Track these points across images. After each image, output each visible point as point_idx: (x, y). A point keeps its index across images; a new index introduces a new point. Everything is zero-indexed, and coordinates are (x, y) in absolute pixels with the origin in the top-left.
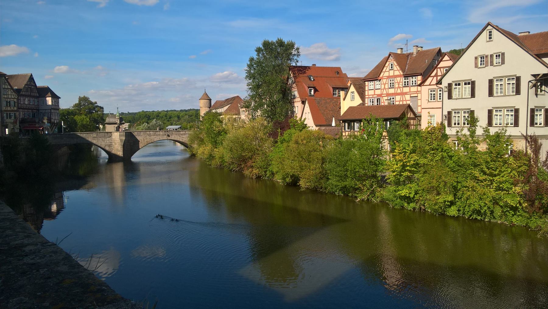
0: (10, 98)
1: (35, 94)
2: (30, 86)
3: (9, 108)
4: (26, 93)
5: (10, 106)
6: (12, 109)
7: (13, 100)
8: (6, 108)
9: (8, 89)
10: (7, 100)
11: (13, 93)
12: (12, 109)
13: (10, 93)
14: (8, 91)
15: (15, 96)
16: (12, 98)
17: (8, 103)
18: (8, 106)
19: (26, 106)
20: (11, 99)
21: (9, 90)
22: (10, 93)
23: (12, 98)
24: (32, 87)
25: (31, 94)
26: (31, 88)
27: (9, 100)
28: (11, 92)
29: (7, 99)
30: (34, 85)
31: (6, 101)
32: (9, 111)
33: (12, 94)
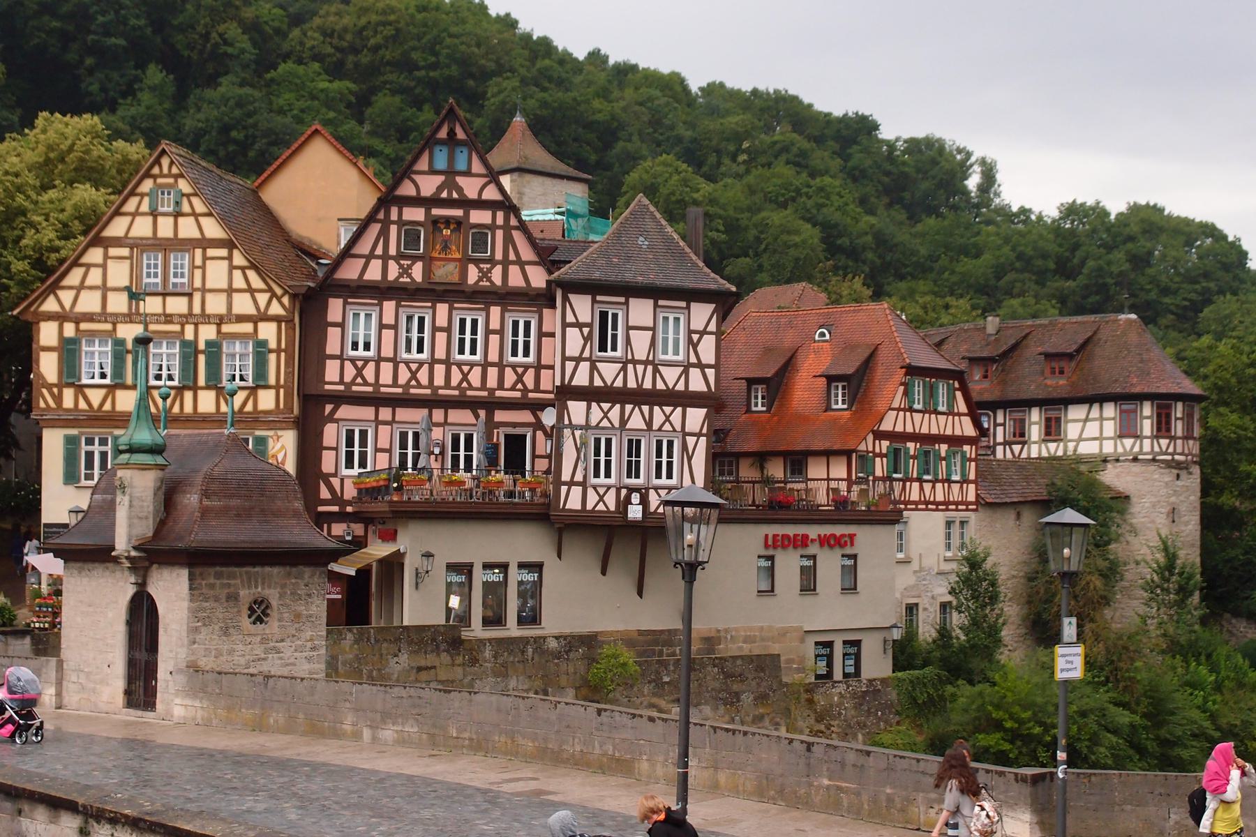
0: (220, 321)
1: (514, 270)
2: (458, 213)
5: (214, 383)
7: (247, 328)
9: (205, 243)
10: (189, 333)
11: (252, 274)
13: (217, 274)
14: (205, 258)
15: (263, 298)
16: (241, 319)
17: (202, 359)
18: (202, 381)
20: (226, 328)
21: (211, 252)
23: (241, 319)
25: (464, 273)
26: (459, 224)
27: (208, 333)
28: (232, 268)
30: (491, 194)
31: (185, 344)
33: (239, 282)
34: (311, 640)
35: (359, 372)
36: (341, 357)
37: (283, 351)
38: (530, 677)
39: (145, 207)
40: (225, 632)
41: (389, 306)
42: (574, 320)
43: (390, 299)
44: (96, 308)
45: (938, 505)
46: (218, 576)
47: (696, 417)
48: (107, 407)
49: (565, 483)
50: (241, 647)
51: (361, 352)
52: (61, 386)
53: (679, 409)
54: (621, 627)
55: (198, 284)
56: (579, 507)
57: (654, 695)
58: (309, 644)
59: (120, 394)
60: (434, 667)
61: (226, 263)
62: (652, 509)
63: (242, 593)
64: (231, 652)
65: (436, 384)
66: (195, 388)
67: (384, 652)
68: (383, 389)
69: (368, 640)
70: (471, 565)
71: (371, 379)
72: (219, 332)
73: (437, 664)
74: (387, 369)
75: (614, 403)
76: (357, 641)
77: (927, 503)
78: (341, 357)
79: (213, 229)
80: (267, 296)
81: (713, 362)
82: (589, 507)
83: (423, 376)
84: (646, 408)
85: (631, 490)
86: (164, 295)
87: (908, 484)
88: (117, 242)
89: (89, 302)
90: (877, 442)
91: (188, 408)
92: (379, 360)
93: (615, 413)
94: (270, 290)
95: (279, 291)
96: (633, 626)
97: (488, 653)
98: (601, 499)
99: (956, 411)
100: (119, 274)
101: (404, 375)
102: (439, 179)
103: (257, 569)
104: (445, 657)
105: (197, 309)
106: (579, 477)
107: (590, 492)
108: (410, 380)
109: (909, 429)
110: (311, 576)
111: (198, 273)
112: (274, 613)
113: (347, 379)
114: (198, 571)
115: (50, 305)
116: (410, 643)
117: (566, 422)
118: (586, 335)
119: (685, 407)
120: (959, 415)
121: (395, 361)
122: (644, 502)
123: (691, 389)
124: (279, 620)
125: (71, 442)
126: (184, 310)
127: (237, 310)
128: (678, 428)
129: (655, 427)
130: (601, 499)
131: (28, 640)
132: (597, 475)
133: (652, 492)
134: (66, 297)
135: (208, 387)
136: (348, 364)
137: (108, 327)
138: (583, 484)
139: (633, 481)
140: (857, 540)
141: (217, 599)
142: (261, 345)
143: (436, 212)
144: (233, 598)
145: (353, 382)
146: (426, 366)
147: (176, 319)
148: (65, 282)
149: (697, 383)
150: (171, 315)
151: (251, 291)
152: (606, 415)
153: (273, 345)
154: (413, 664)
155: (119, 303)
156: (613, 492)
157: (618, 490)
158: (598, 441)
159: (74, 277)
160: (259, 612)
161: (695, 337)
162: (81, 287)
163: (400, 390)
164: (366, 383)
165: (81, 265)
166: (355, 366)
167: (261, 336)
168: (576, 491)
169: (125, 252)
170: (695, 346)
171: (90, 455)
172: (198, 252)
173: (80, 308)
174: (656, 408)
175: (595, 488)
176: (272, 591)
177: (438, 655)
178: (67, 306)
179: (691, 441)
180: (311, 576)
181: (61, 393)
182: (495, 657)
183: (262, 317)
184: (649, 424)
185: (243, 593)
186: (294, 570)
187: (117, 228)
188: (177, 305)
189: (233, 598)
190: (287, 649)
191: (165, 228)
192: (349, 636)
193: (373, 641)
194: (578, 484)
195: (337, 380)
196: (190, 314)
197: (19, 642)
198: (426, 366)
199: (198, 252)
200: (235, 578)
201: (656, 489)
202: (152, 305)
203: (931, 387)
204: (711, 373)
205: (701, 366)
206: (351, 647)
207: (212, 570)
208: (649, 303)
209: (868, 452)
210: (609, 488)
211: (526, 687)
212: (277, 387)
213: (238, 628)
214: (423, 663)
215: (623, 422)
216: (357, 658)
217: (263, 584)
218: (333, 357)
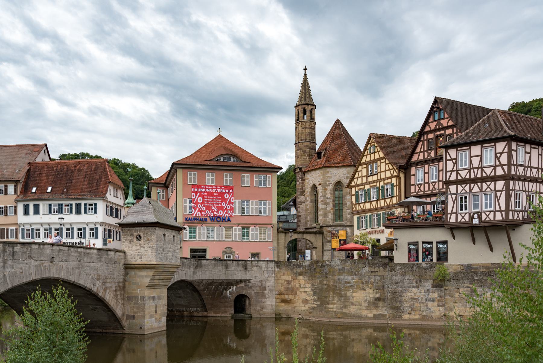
0: (384, 180)
3: (382, 202)
4: (429, 154)
6: (388, 203)
7: (389, 181)
8: (377, 203)
11: (390, 165)
12: (388, 203)
13: (383, 167)
14: (381, 163)
15: (392, 171)
16: (388, 178)
19: (431, 189)
20: (386, 182)
22: (383, 167)
23: (388, 178)
24: (449, 131)
27: (382, 184)
28: (386, 164)
29: (378, 183)
32: (381, 208)
34: (152, 245)
35: (420, 188)
36: (414, 185)
37: (397, 185)
38: (414, 276)
39: (368, 153)
40: (130, 242)
41: (427, 166)
42: (450, 158)
43: (427, 164)
44: (361, 183)
46: (128, 230)
47: (500, 184)
48: (364, 208)
49: (449, 214)
50: (134, 246)
51: (420, 182)
52: (356, 204)
53: (493, 183)
55: (379, 171)
56: (454, 221)
58: (151, 246)
59: (366, 204)
60: (377, 272)
61: (384, 163)
62: (483, 219)
63: (134, 234)
64: (132, 247)
65: (440, 188)
66: (380, 200)
67: (360, 267)
68: (426, 192)
69: (355, 263)
71: (423, 190)
72: (384, 183)
73: (378, 270)
74: (427, 185)
75: (467, 184)
76: (351, 263)
78: (414, 185)
79: (382, 155)
80: (393, 170)
81: (507, 163)
82: (459, 220)
83: (436, 186)
84: (479, 184)
85: (474, 213)
86: (373, 175)
88: (364, 164)
89: (359, 182)
91: (379, 206)
92: (425, 183)
93: (467, 188)
94: (394, 168)
95: (395, 168)
97: (398, 268)
98: (463, 217)
100: (365, 172)
101: (431, 187)
102: (436, 123)
103: (138, 228)
104: (381, 269)
105: (379, 178)
106: (454, 211)
107: (459, 215)
108: (433, 188)
110: (152, 229)
111: (379, 167)
112: (142, 238)
113: (417, 191)
114: (124, 229)
115: (353, 184)
116: (369, 264)
117: (449, 193)
118: (454, 162)
121: (429, 183)
122: (480, 217)
123: (497, 174)
124: (144, 240)
125: (358, 218)
126: (377, 179)
127: (387, 176)
128: (493, 189)
129: (484, 190)
130: (463, 217)
131: (274, 263)
132: (462, 209)
133: (483, 214)
134: (355, 180)
135: (382, 199)
136: (416, 186)
137: (363, 187)
138: (456, 213)
139: (476, 210)
141: (128, 235)
142: (392, 184)
143: (437, 133)
144: (132, 235)
145: (418, 192)
146: (437, 183)
147: (375, 181)
148: (355, 177)
149: (500, 172)
150: (374, 181)
151: (390, 170)
152: (464, 189)
153: (395, 184)
154: (370, 270)
155: (365, 180)
156: (467, 215)
157: (470, 214)
158: (461, 198)
159: (356, 176)
160: (139, 238)
161: (498, 155)
162: (358, 177)
163: (430, 192)
164: (421, 191)
165: (358, 172)
166: (418, 186)
167: (392, 182)
168: (454, 216)
169: (365, 166)
170: (499, 159)
171: (362, 221)
172: (379, 162)
173: (358, 183)
174: (484, 184)
175: (460, 214)
176: (142, 233)
177: (379, 268)
178: (356, 183)
179: (498, 194)
180: (152, 229)
181: (356, 206)
182: (401, 269)
183: (392, 177)
184: (481, 190)
185: (134, 234)
186: (147, 228)
187: (363, 161)
188: (375, 177)
189: (132, 235)
190: (146, 247)
191: (373, 158)
192: (349, 262)
193: (356, 263)
194: (454, 213)
195: (414, 192)
196: (378, 180)
197: (271, 263)
198: (437, 183)
199: (379, 162)
200: (132, 230)
201: (485, 212)
202: (370, 179)
204: (506, 168)
205: (501, 165)
206: (349, 265)
207: (127, 228)
210: (466, 213)
211: (412, 279)
212: (396, 196)
213: (133, 242)
214: (373, 270)
215: (471, 190)
216: (351, 268)
217: (139, 232)
218: (413, 185)
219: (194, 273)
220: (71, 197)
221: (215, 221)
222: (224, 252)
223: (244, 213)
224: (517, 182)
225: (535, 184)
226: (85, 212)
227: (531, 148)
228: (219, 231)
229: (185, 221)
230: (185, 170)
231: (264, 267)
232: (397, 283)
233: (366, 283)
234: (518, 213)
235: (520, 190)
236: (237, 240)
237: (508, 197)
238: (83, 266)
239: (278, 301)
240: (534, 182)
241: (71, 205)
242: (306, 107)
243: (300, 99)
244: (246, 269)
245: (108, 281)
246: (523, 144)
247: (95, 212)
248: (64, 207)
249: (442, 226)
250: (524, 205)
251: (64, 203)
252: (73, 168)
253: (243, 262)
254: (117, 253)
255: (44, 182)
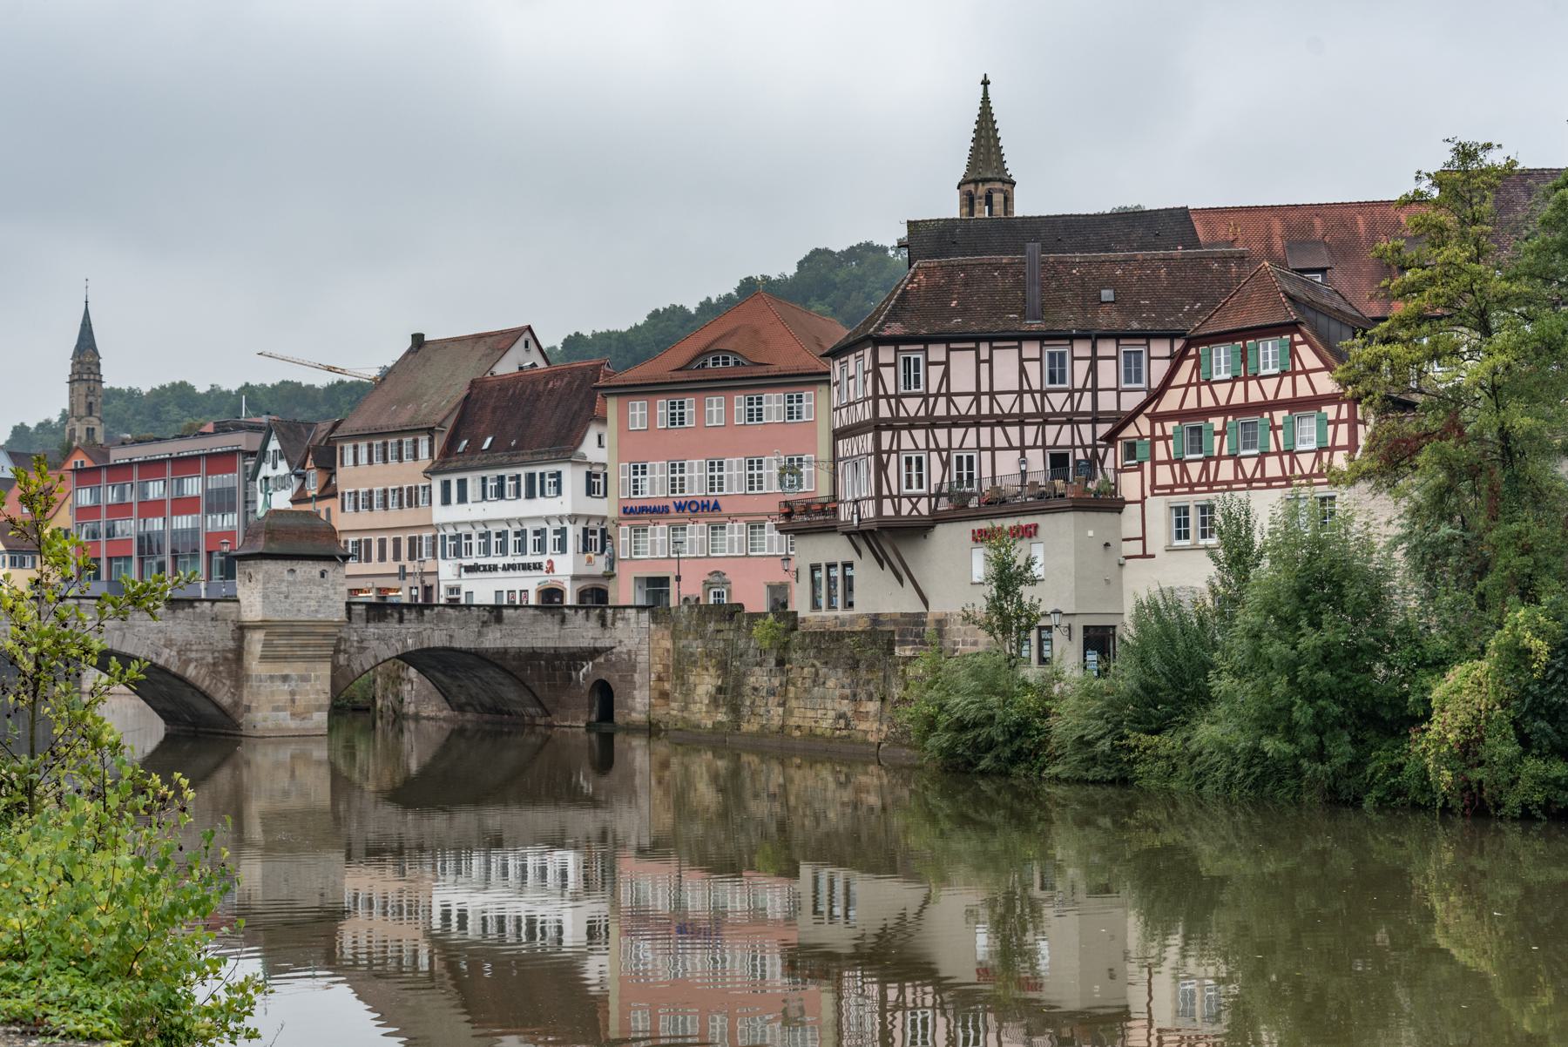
45: (1269, 483)
54: (892, 611)
57: (815, 657)
70: (820, 565)
77: (1249, 482)
87: (1213, 464)
90: (1158, 426)
96: (899, 610)
99: (1298, 367)
104: (727, 626)
109: (1208, 402)
119: (866, 432)
120: (1306, 372)
140: (1041, 531)
203: (1244, 351)
208: (891, 349)
209: (1141, 437)
214: (719, 627)
219: (480, 634)
220: (519, 459)
221: (687, 510)
222: (705, 582)
223: (751, 488)
224: (905, 434)
225: (972, 431)
226: (542, 494)
227: (949, 350)
228: (696, 533)
229: (623, 515)
230: (624, 399)
231: (632, 620)
232: (741, 656)
233: (709, 655)
234: (914, 500)
235: (917, 448)
236: (736, 553)
237: (881, 468)
238: (131, 627)
239: (656, 694)
240: (967, 426)
241: (518, 477)
242: (971, 187)
243: (973, 163)
244: (604, 625)
245: (194, 648)
246: (922, 347)
247: (559, 492)
248: (507, 482)
249: (829, 529)
250: (936, 479)
251: (507, 472)
252: (541, 388)
253: (598, 611)
254: (218, 604)
255: (483, 426)
